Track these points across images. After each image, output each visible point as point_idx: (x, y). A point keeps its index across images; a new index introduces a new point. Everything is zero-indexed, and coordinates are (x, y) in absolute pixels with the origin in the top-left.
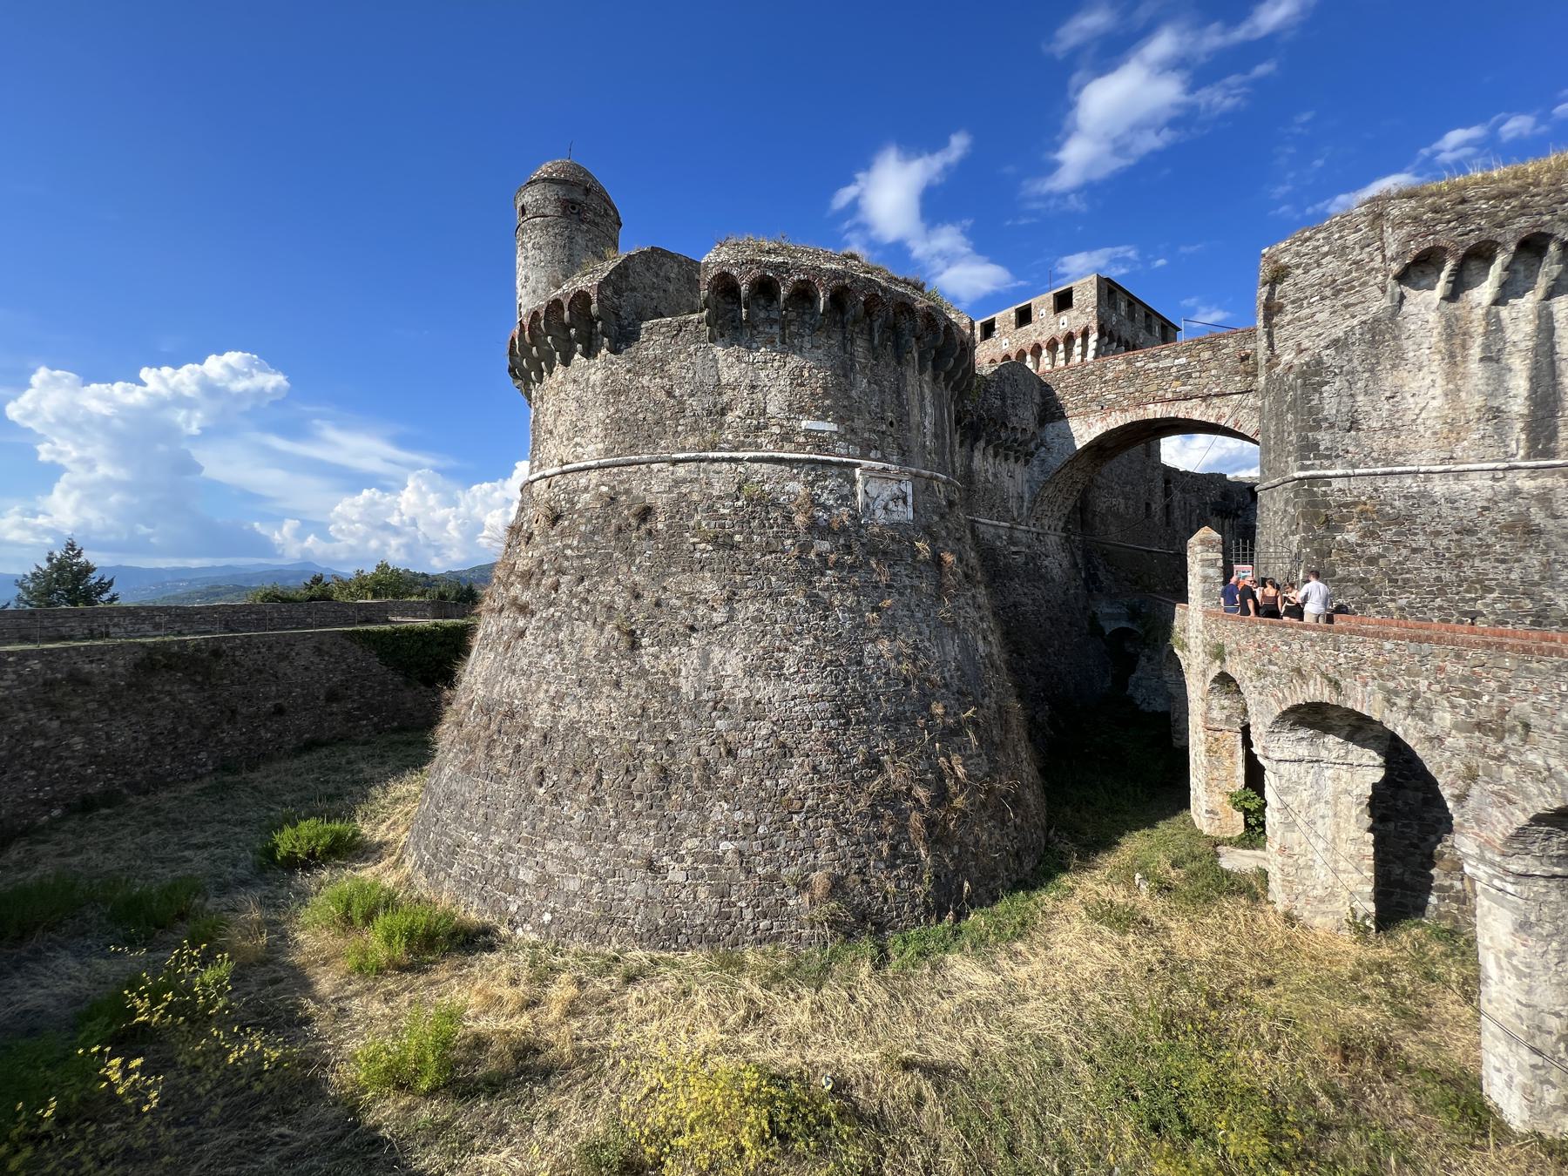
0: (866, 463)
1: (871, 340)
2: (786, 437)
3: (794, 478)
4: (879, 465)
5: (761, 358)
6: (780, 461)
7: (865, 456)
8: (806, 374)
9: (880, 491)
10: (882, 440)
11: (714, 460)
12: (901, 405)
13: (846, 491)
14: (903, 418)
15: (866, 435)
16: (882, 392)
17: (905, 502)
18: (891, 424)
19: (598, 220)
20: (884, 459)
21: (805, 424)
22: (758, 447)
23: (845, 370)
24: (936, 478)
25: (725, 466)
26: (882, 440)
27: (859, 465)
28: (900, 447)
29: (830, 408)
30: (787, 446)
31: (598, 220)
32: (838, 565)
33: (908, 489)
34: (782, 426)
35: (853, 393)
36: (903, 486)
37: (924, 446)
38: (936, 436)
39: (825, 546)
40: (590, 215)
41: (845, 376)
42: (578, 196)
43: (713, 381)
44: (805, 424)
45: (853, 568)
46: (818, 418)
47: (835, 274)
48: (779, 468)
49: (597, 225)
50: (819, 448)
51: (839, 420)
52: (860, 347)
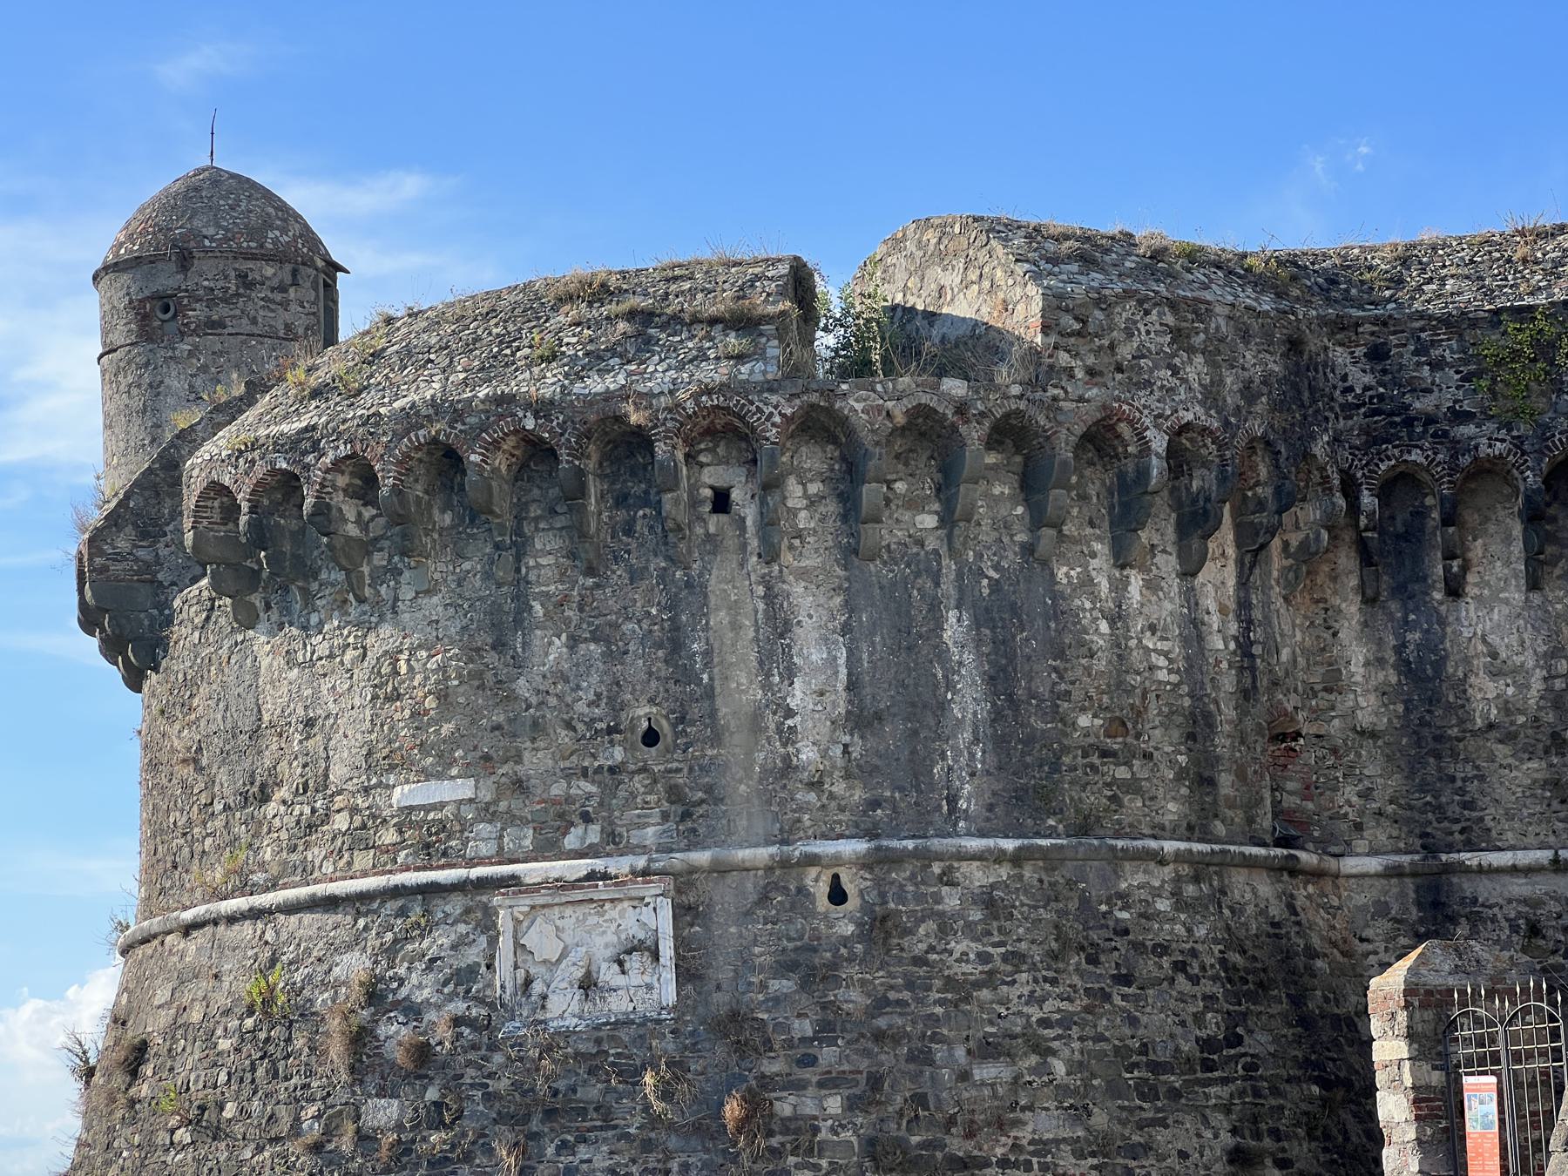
0: (532, 871)
1: (578, 532)
2: (359, 839)
3: (357, 941)
4: (582, 866)
5: (323, 649)
6: (331, 903)
7: (548, 849)
8: (403, 669)
9: (588, 946)
10: (609, 791)
11: (232, 919)
12: (686, 675)
13: (473, 955)
15: (557, 790)
16: (615, 656)
17: (656, 956)
18: (651, 738)
19: (221, 311)
20: (613, 842)
21: (405, 794)
22: (307, 873)
23: (501, 630)
24: (812, 860)
25: (246, 930)
26: (609, 791)
27: (513, 881)
28: (674, 794)
29: (454, 741)
30: (363, 860)
31: (221, 311)
33: (663, 921)
34: (354, 810)
35: (522, 687)
36: (646, 914)
37: (788, 767)
38: (860, 719)
39: (384, 1112)
40: (197, 313)
41: (499, 646)
42: (167, 280)
43: (247, 724)
44: (405, 794)
46: (427, 775)
47: (410, 419)
48: (331, 919)
49: (215, 325)
50: (429, 852)
51: (485, 764)
52: (546, 558)
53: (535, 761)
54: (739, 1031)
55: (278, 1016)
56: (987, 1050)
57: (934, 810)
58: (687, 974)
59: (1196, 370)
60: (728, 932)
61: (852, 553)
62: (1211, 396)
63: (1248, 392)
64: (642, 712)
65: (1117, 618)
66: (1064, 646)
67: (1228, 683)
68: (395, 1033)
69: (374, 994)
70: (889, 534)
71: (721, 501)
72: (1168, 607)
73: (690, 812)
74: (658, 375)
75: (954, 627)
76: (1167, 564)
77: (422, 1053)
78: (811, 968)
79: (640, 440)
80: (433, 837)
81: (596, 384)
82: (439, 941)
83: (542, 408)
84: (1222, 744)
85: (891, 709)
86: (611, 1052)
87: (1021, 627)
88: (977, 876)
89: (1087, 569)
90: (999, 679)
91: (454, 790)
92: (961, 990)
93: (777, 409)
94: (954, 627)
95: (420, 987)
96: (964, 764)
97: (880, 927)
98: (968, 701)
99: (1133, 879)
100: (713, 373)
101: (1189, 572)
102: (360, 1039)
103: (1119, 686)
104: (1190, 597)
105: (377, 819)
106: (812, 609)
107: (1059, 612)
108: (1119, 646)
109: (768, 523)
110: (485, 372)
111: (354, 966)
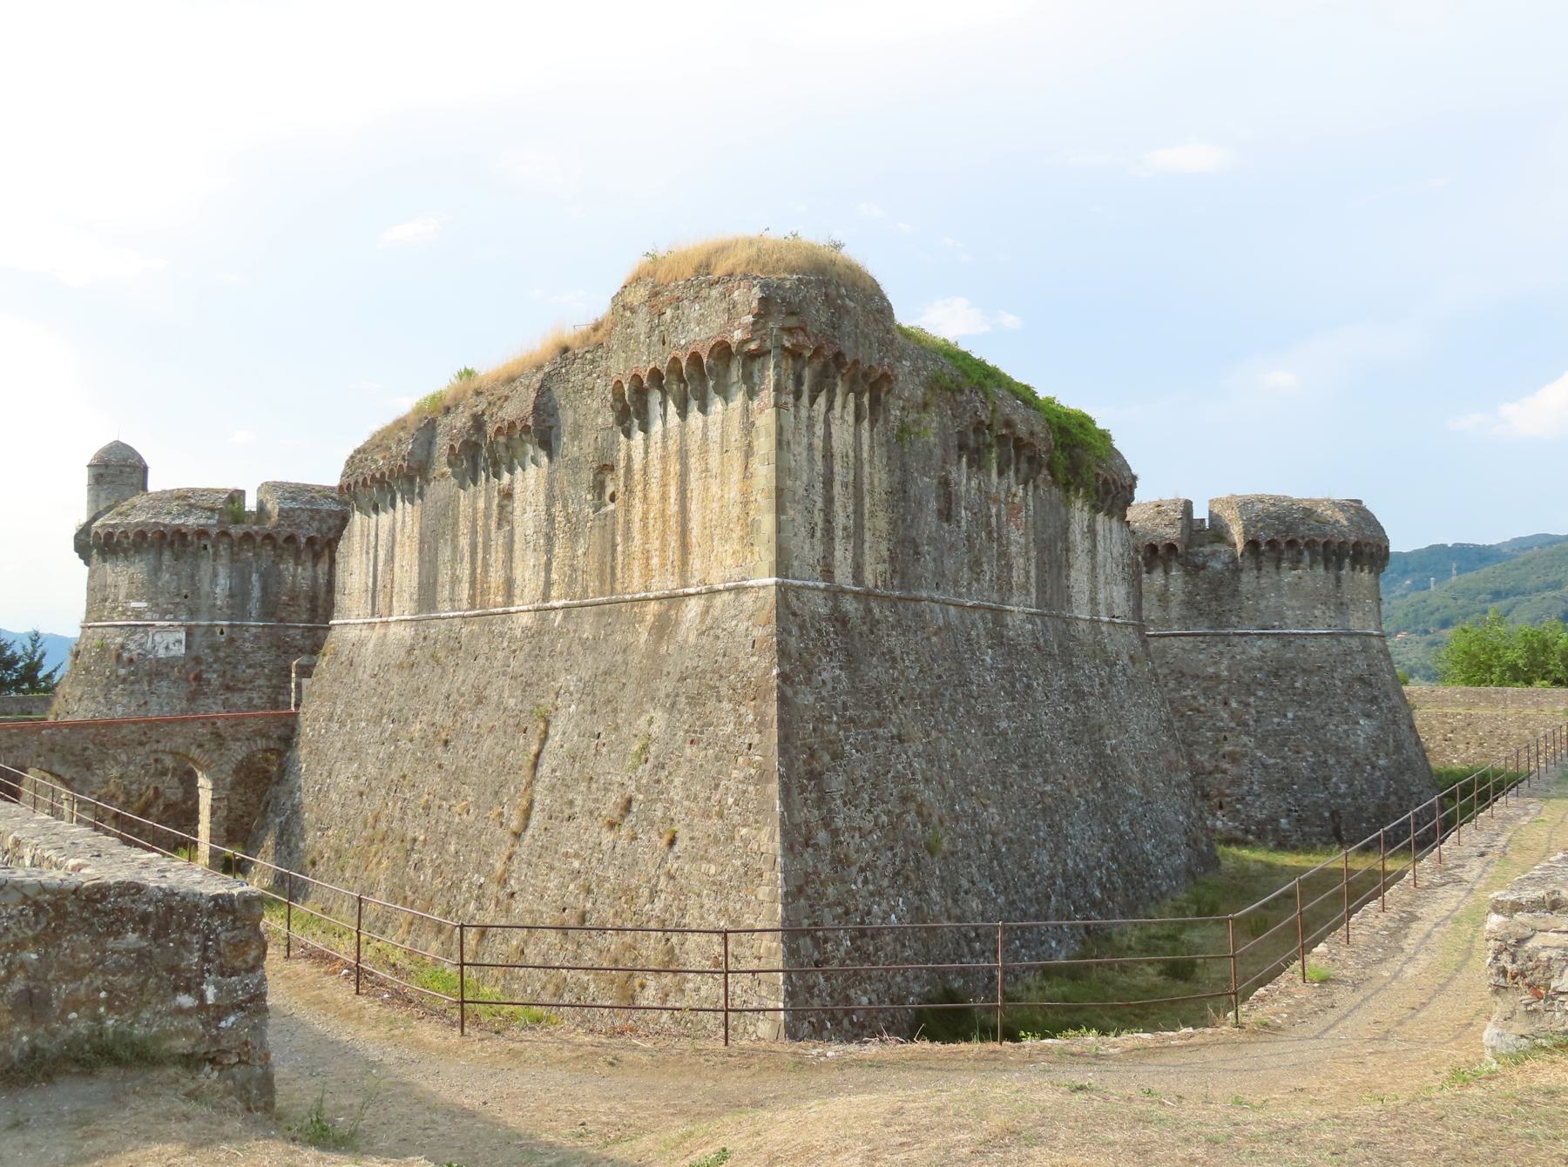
2: (123, 613)
9: (169, 641)
14: (196, 591)
20: (175, 619)
21: (134, 604)
22: (112, 619)
23: (156, 571)
32: (124, 681)
33: (182, 636)
38: (231, 596)
39: (122, 672)
42: (102, 471)
44: (134, 604)
45: (132, 683)
50: (138, 617)
53: (161, 600)
54: (198, 660)
55: (103, 648)
56: (250, 666)
57: (245, 615)
58: (187, 647)
59: (315, 524)
60: (197, 639)
61: (232, 561)
62: (319, 530)
63: (330, 529)
64: (184, 591)
65: (294, 576)
66: (280, 580)
67: (323, 589)
68: (126, 655)
69: (123, 647)
70: (243, 557)
71: (205, 547)
72: (309, 573)
73: (193, 613)
74: (191, 521)
75: (255, 577)
76: (309, 565)
77: (131, 661)
78: (215, 648)
79: (184, 536)
80: (138, 614)
81: (177, 522)
82: (137, 637)
83: (165, 526)
84: (320, 602)
85: (238, 596)
86: (170, 663)
87: (270, 579)
88: (254, 630)
89: (288, 567)
90: (264, 589)
91: (143, 604)
92: (246, 654)
93: (214, 532)
94: (255, 577)
95: (132, 646)
96: (254, 606)
97: (231, 640)
98: (256, 593)
99: (291, 632)
100: (202, 521)
101: (315, 565)
102: (119, 657)
103: (293, 590)
104: (315, 572)
105: (127, 609)
106: (223, 572)
107: (280, 574)
108: (294, 582)
109: (215, 554)
110: (155, 515)
111: (119, 640)
